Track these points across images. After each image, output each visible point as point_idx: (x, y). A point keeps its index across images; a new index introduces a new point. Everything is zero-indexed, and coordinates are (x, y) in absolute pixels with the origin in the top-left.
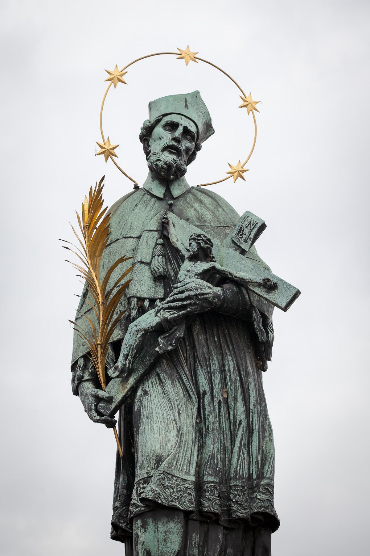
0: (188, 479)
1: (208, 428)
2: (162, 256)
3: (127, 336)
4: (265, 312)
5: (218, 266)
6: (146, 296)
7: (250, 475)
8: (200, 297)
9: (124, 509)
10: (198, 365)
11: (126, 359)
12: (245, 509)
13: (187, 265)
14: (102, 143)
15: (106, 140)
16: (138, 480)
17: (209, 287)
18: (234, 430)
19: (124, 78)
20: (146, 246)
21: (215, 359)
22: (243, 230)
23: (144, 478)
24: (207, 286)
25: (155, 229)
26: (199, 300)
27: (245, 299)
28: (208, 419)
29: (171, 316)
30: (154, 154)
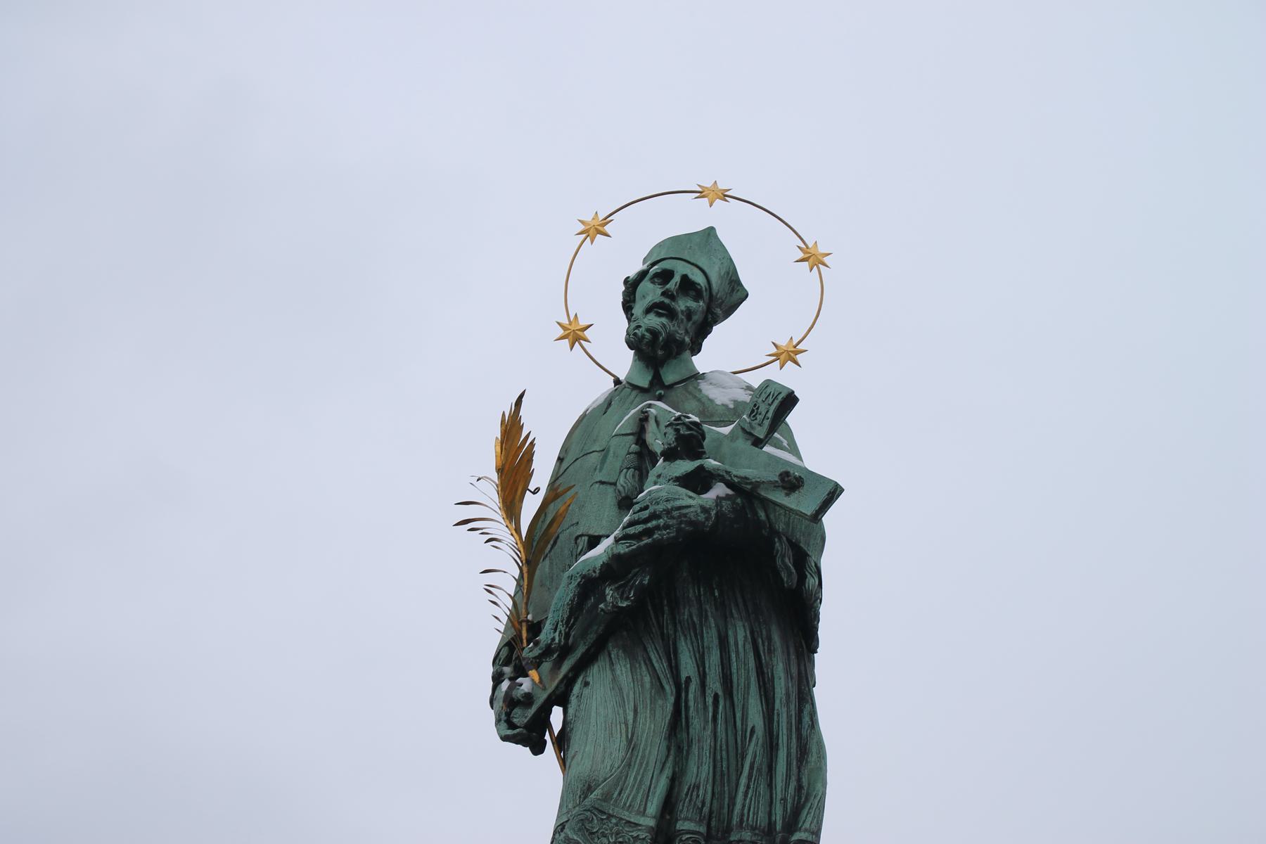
0: (641, 823)
2: (633, 470)
4: (800, 542)
5: (711, 463)
6: (601, 534)
7: (771, 825)
8: (676, 513)
10: (681, 634)
11: (555, 630)
14: (565, 321)
15: (572, 318)
17: (690, 497)
18: (742, 744)
19: (607, 228)
21: (713, 625)
22: (758, 409)
24: (686, 495)
25: (629, 432)
26: (673, 518)
27: (758, 519)
29: (627, 550)
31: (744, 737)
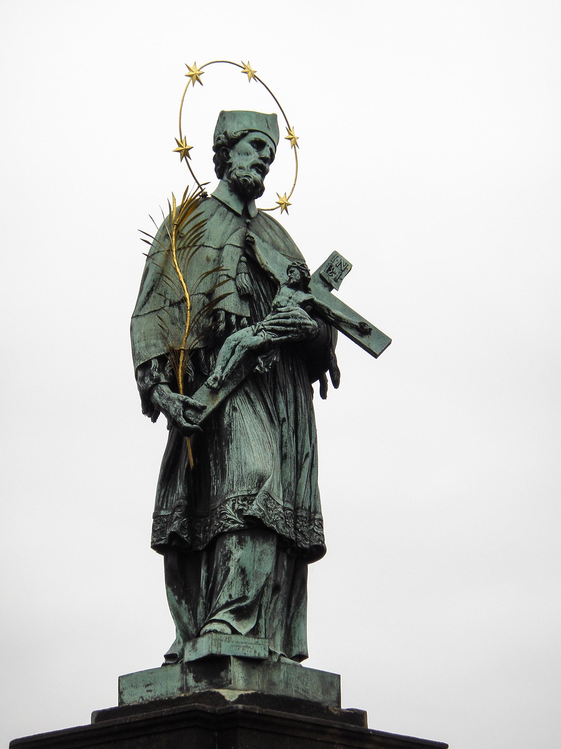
0: (280, 504)
1: (286, 456)
3: (225, 350)
6: (233, 311)
8: (303, 326)
9: (185, 520)
10: (279, 391)
11: (223, 372)
12: (307, 541)
13: (285, 291)
14: (179, 140)
16: (235, 496)
20: (231, 261)
22: (333, 269)
23: (244, 495)
25: (239, 245)
26: (301, 328)
28: (285, 446)
29: (274, 339)
30: (240, 168)
31: (301, 459)
